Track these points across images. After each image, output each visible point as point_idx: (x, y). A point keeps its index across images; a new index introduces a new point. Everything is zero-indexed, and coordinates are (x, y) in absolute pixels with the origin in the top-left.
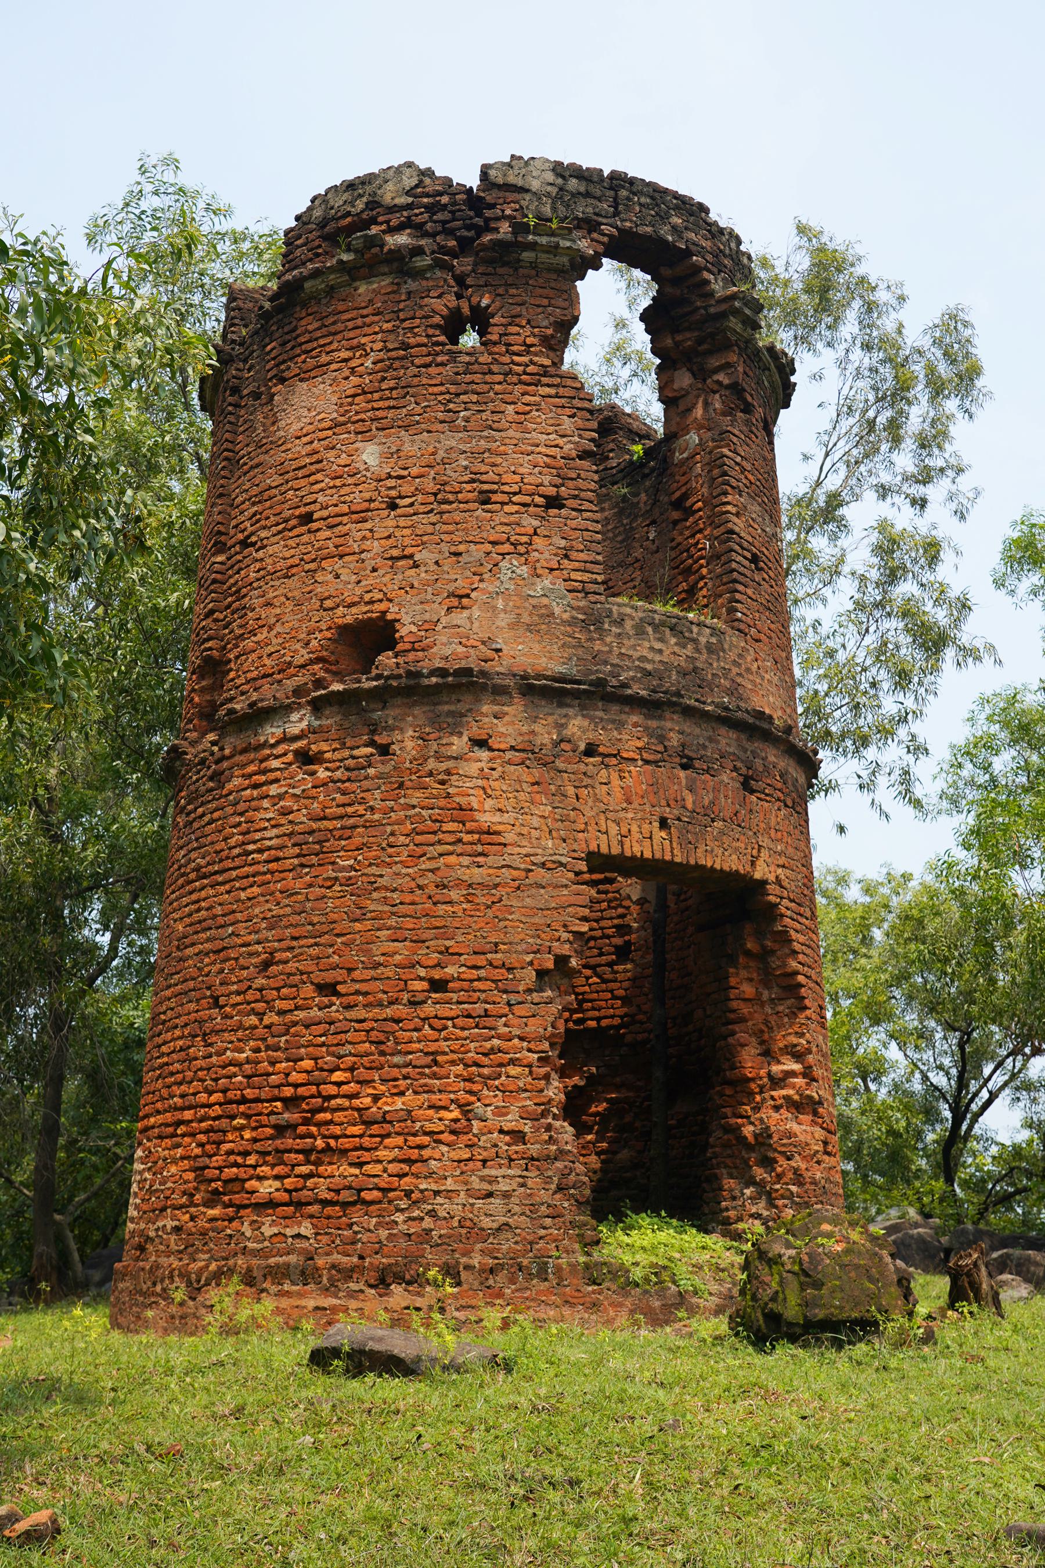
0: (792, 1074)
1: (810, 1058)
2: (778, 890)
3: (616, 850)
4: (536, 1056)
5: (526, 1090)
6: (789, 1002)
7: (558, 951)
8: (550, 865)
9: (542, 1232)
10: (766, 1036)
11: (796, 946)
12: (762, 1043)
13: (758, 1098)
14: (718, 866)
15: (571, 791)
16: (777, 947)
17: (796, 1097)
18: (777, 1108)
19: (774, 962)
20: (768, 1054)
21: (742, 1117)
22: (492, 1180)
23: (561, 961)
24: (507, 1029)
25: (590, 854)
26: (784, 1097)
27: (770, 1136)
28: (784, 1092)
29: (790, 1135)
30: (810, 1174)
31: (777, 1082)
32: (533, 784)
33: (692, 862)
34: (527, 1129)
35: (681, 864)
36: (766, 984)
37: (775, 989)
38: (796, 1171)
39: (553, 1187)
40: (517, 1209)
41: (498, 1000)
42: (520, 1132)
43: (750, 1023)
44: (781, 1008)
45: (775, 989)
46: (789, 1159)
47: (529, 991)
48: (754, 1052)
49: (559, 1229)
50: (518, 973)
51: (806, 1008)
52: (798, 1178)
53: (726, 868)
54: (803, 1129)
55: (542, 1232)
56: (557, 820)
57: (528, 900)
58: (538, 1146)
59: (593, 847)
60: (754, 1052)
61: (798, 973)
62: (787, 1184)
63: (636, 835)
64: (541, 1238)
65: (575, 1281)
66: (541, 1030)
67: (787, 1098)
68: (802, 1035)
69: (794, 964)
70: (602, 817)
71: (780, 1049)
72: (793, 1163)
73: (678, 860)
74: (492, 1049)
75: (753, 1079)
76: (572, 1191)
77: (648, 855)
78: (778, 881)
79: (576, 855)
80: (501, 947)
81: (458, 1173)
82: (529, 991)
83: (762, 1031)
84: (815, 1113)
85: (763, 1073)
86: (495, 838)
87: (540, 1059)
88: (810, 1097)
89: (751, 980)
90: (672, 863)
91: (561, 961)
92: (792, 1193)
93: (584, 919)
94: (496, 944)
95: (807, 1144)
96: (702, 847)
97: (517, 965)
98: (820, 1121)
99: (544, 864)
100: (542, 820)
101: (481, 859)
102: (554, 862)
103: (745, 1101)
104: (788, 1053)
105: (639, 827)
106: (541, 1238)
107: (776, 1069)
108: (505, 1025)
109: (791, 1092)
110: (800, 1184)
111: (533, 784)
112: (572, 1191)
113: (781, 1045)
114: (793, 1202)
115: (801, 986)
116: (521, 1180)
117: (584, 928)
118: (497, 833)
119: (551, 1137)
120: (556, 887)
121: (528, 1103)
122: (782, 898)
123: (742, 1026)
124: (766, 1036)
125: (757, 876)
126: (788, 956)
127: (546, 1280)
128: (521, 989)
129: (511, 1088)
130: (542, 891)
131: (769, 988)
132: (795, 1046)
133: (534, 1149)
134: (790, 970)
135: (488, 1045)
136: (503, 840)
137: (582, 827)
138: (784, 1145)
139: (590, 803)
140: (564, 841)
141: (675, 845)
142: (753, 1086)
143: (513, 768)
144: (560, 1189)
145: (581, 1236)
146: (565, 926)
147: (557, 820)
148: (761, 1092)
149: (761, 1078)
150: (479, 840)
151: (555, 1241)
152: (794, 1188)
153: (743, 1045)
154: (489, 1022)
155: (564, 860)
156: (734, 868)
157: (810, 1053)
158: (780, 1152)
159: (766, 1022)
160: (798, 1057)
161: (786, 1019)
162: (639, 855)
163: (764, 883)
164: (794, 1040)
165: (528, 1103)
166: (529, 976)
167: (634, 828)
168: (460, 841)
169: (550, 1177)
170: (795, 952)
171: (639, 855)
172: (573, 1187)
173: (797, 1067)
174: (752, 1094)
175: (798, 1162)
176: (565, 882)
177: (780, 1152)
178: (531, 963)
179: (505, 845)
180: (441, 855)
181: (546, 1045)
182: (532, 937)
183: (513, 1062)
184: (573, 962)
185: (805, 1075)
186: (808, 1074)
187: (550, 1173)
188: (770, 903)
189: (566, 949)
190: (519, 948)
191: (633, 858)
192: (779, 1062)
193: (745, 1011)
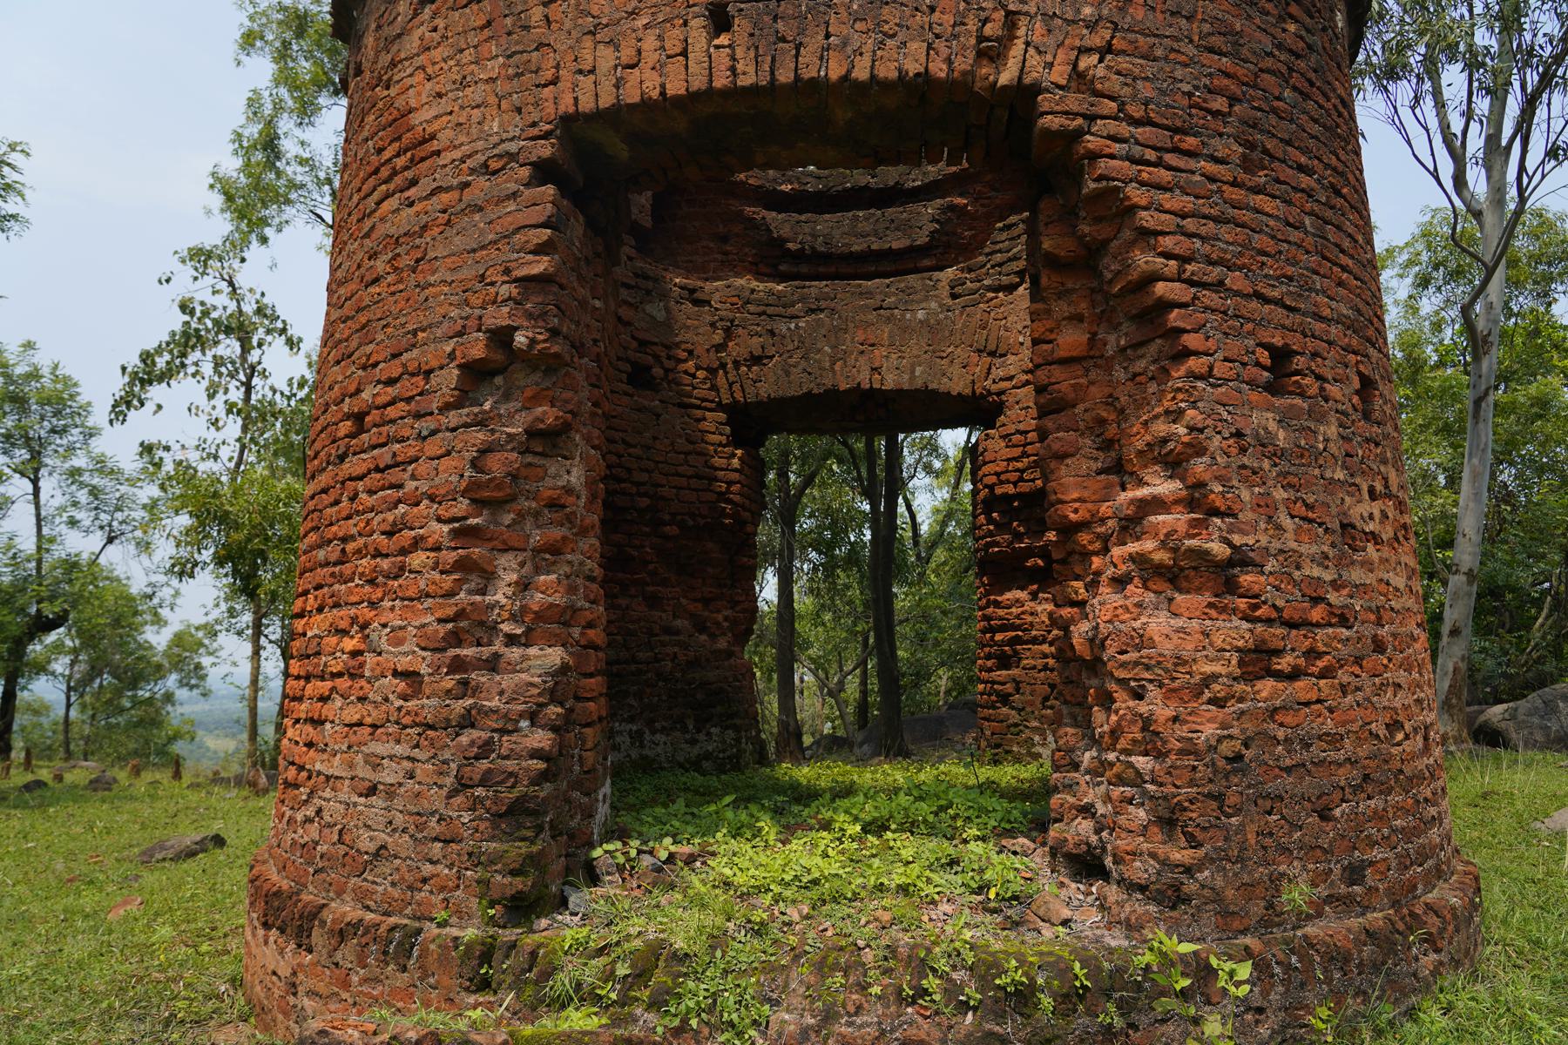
0: (1157, 504)
1: (1199, 466)
2: (1074, 102)
3: (606, 101)
4: (446, 528)
5: (428, 595)
6: (1153, 349)
7: (489, 322)
8: (494, 165)
9: (428, 869)
10: (1112, 430)
11: (1147, 219)
12: (1107, 445)
13: (1097, 562)
14: (861, 73)
15: (537, 13)
16: (1104, 231)
17: (1162, 556)
18: (1120, 582)
19: (1109, 266)
20: (1120, 471)
21: (1073, 604)
22: (375, 763)
23: (500, 337)
24: (415, 483)
25: (567, 121)
26: (1132, 558)
27: (1103, 646)
28: (1133, 547)
29: (1142, 641)
30: (1182, 731)
31: (1131, 525)
32: (482, 28)
33: (785, 76)
34: (424, 670)
35: (754, 90)
36: (1106, 318)
37: (1125, 327)
38: (1147, 723)
39: (449, 781)
40: (399, 819)
41: (406, 432)
42: (416, 674)
43: (1080, 409)
44: (1141, 365)
45: (1125, 327)
46: (1139, 696)
47: (446, 408)
48: (1086, 466)
49: (451, 866)
50: (434, 380)
51: (1188, 353)
52: (1151, 742)
53: (887, 71)
54: (1167, 625)
55: (428, 869)
56: (510, 78)
57: (457, 239)
58: (434, 702)
59: (566, 105)
60: (1086, 466)
61: (1153, 278)
62: (1128, 752)
63: (651, 57)
64: (425, 881)
65: (446, 981)
66: (454, 478)
67: (1139, 559)
68: (1175, 416)
69: (1144, 260)
70: (588, 42)
71: (1140, 453)
72: (1143, 708)
73: (743, 81)
74: (394, 523)
75: (1083, 525)
76: (479, 792)
77: (675, 88)
78: (1078, 77)
79: (535, 131)
80: (421, 335)
81: (344, 748)
82: (446, 408)
83: (1102, 422)
84: (1231, 587)
85: (1104, 508)
86: (435, 146)
87: (455, 534)
88: (1203, 554)
89: (1077, 318)
90: (734, 93)
91: (500, 337)
92: (1137, 772)
93: (539, 250)
94: (415, 333)
95: (1180, 661)
96: (814, 42)
97: (434, 363)
98: (1242, 603)
99: (485, 165)
100: (488, 87)
101: (412, 192)
102: (500, 156)
103: (1078, 570)
104: (1155, 461)
105: (660, 38)
106: (425, 881)
107: (1124, 497)
108: (413, 477)
109: (1148, 545)
110: (1160, 755)
111: (482, 28)
112: (479, 792)
113: (1140, 445)
114: (1145, 793)
115: (1166, 305)
116: (407, 764)
117: (540, 265)
118: (433, 137)
119: (465, 683)
120: (500, 201)
121: (429, 619)
122: (1092, 118)
123: (1062, 418)
124: (1112, 430)
125: (1005, 78)
126: (1131, 244)
127: (404, 969)
128: (435, 406)
129: (410, 593)
130: (477, 217)
131: (1116, 327)
132: (1165, 441)
133: (427, 706)
134: (1134, 275)
135: (390, 517)
136: (435, 146)
137: (549, 74)
138: (1123, 665)
139: (568, 24)
140: (519, 110)
141: (739, 53)
142: (1084, 538)
143: (457, 14)
144: (462, 785)
145: (484, 883)
146: (507, 271)
147: (510, 78)
148: (1105, 550)
149: (1103, 520)
150: (412, 160)
151: (442, 889)
152: (1141, 762)
153: (1061, 457)
154: (394, 475)
155: (513, 147)
156: (913, 68)
157: (1200, 451)
158: (1122, 682)
159: (1111, 401)
160: (1174, 465)
161: (1153, 387)
162: (655, 94)
163: (1025, 94)
164: (1161, 428)
165: (429, 619)
166: (449, 377)
167: (650, 43)
168: (395, 173)
169: (445, 762)
170: (1146, 234)
171: (655, 94)
172: (483, 782)
173: (1162, 486)
174: (1086, 555)
175: (1157, 706)
176: (512, 187)
177: (1122, 682)
178: (452, 356)
179: (438, 153)
180: (379, 203)
181: (462, 506)
182: (458, 306)
183: (417, 544)
184: (520, 339)
185: (1191, 504)
186: (1195, 500)
187: (447, 755)
188: (1047, 132)
189: (499, 317)
190: (439, 332)
191: (646, 104)
192: (1141, 483)
193: (1064, 387)
